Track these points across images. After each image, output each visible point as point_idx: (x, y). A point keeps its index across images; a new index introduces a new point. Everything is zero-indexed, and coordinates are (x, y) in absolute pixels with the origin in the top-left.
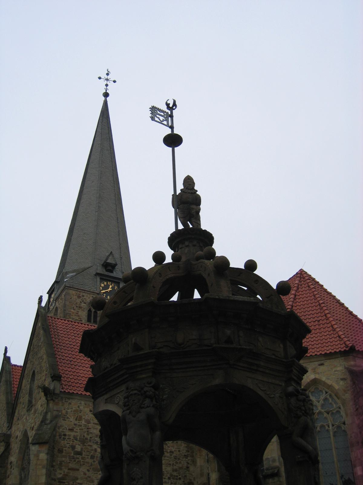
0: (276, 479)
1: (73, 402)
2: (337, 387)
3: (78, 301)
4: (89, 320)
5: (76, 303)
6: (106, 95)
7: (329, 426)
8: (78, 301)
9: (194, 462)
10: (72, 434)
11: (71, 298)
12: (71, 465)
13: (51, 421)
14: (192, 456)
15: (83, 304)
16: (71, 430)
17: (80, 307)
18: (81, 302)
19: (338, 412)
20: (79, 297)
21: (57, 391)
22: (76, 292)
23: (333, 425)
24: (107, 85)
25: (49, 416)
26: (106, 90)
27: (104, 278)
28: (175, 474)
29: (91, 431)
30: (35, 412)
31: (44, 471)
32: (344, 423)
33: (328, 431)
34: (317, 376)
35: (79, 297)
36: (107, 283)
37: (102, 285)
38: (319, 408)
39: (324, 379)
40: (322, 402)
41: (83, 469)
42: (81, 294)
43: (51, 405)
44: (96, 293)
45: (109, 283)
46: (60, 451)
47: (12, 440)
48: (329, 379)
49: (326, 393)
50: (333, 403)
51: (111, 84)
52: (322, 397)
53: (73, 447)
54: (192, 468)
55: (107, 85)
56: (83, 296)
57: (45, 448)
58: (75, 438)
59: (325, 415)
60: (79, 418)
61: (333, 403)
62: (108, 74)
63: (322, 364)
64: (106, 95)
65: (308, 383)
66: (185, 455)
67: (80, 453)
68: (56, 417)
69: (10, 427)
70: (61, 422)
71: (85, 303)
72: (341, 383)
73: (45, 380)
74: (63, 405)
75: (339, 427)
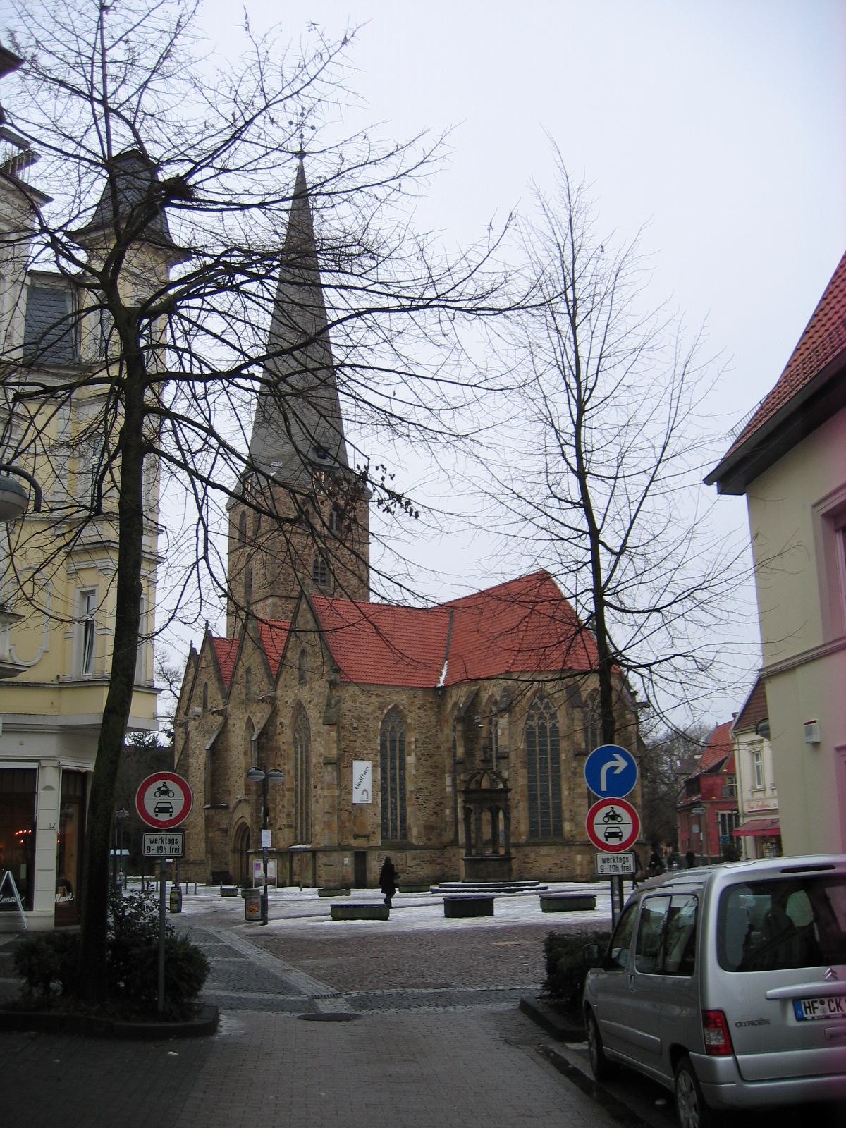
0: (506, 760)
1: (349, 688)
9: (442, 731)
10: (350, 714)
12: (351, 738)
13: (335, 705)
14: (440, 725)
21: (338, 682)
25: (333, 701)
28: (427, 740)
29: (364, 710)
30: (311, 689)
31: (335, 745)
41: (360, 740)
43: (334, 692)
46: (343, 728)
53: (352, 724)
54: (440, 735)
57: (335, 727)
58: (353, 717)
60: (355, 701)
67: (356, 728)
68: (338, 702)
69: (275, 689)
70: (342, 705)
75: (554, 725)
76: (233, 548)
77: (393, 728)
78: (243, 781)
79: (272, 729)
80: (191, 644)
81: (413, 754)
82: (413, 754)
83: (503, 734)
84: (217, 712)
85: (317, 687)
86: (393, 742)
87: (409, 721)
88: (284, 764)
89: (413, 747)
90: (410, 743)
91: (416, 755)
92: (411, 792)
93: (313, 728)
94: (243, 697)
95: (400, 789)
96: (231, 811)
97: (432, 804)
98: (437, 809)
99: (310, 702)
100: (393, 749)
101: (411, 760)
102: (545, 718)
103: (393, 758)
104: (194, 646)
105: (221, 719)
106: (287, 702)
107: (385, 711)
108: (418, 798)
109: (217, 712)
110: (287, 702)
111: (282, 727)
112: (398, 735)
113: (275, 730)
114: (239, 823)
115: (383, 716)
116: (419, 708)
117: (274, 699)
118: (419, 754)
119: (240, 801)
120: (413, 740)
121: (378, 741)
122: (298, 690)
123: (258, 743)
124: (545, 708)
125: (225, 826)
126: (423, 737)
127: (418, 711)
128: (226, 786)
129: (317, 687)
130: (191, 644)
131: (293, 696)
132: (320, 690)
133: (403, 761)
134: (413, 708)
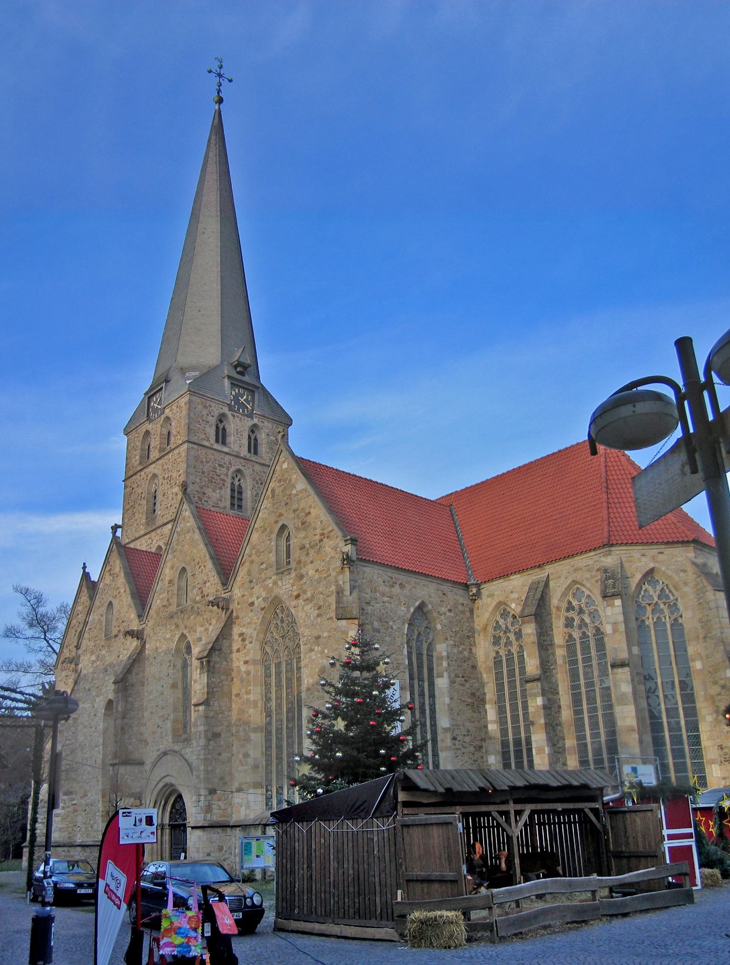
2: (677, 579)
3: (205, 412)
4: (217, 441)
5: (203, 416)
6: (220, 101)
7: (665, 619)
8: (205, 412)
11: (195, 408)
15: (210, 418)
16: (368, 603)
17: (208, 422)
18: (208, 415)
19: (675, 604)
20: (205, 407)
22: (202, 400)
23: (670, 618)
24: (220, 85)
26: (218, 93)
27: (236, 383)
32: (681, 616)
33: (664, 623)
34: (657, 565)
35: (205, 407)
36: (239, 391)
37: (233, 393)
38: (656, 599)
39: (663, 569)
40: (658, 592)
42: (208, 403)
44: (226, 403)
45: (242, 391)
47: (233, 606)
48: (668, 569)
49: (663, 583)
50: (670, 595)
51: (225, 83)
52: (659, 588)
53: (372, 624)
55: (220, 85)
56: (210, 406)
59: (662, 606)
61: (670, 595)
62: (221, 67)
63: (661, 553)
64: (220, 101)
65: (647, 572)
66: (468, 636)
67: (378, 631)
71: (213, 416)
72: (682, 574)
73: (322, 540)
74: (358, 574)
75: (676, 620)
76: (131, 473)
77: (419, 634)
78: (169, 724)
79: (226, 643)
80: (84, 567)
81: (445, 674)
82: (445, 674)
83: (615, 631)
84: (130, 633)
85: (311, 572)
86: (420, 655)
87: (439, 627)
88: (248, 693)
89: (445, 664)
90: (440, 658)
91: (449, 677)
92: (446, 730)
93: (305, 632)
94: (173, 608)
95: (431, 725)
96: (147, 767)
97: (472, 749)
98: (477, 755)
99: (298, 597)
100: (420, 667)
101: (442, 683)
102: (662, 611)
103: (421, 680)
104: (87, 570)
105: (133, 644)
106: (252, 604)
107: (412, 610)
108: (454, 739)
109: (130, 633)
110: (252, 604)
111: (244, 640)
112: (425, 646)
113: (230, 646)
114: (161, 784)
115: (409, 616)
116: (450, 611)
117: (228, 601)
118: (453, 675)
119: (165, 754)
120: (444, 654)
121: (406, 653)
122: (275, 583)
123: (209, 662)
124: (659, 597)
125: (138, 790)
126: (455, 651)
127: (448, 614)
128: (142, 734)
129: (311, 572)
130: (84, 567)
131: (264, 594)
132: (317, 576)
133: (432, 684)
134: (443, 609)
